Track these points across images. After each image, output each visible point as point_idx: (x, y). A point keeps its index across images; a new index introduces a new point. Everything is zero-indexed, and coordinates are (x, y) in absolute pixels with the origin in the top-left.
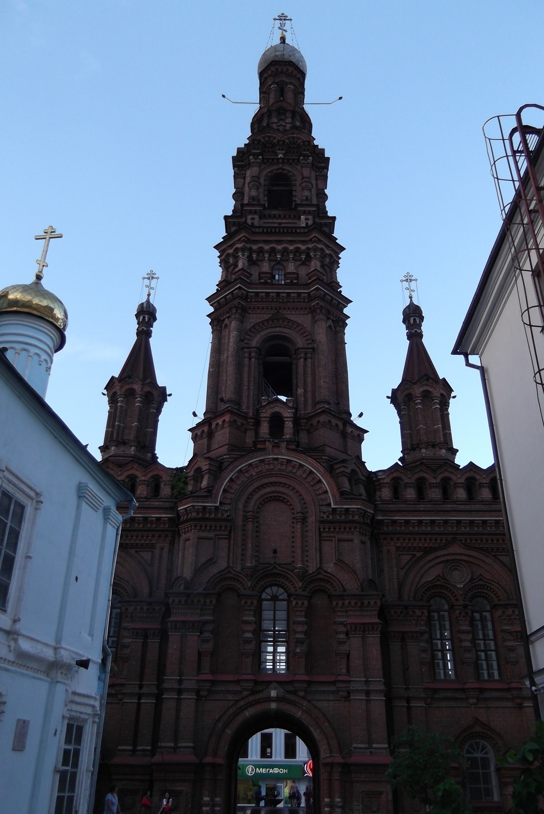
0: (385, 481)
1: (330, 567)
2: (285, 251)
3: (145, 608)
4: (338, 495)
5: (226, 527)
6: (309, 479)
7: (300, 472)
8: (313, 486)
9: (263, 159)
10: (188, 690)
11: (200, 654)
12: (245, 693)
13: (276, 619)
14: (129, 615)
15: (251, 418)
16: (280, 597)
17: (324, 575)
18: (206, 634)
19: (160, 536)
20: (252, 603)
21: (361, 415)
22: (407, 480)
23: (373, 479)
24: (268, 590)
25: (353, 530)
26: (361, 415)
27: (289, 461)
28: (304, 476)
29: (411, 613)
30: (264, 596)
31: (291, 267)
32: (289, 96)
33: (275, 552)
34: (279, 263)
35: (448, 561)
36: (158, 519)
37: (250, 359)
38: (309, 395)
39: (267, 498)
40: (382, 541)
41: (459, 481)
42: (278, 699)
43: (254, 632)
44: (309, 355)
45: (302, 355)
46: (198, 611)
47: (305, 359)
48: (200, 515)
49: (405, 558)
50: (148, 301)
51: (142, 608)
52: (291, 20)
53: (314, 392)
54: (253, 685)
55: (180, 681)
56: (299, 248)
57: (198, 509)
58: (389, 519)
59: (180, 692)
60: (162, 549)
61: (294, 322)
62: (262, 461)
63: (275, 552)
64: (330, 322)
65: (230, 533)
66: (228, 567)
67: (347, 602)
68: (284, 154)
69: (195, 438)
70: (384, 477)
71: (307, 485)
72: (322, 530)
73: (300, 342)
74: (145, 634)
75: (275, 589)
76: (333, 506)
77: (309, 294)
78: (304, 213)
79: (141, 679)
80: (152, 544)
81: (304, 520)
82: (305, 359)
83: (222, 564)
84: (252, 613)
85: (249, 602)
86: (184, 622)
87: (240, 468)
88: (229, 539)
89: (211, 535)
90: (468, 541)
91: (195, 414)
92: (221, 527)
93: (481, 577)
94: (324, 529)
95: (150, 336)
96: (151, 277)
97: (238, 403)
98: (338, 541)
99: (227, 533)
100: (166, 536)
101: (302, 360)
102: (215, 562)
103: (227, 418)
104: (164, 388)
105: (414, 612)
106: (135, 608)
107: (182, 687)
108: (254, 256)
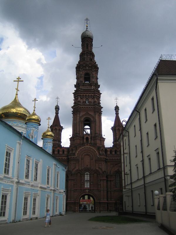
1: (97, 169)
11: (74, 185)
21: (104, 136)
23: (106, 150)
26: (104, 136)
31: (90, 100)
32: (89, 48)
34: (87, 99)
36: (64, 159)
42: (88, 192)
49: (112, 166)
50: (57, 105)
52: (89, 20)
55: (71, 189)
63: (87, 166)
69: (70, 140)
73: (92, 119)
83: (77, 168)
96: (58, 98)
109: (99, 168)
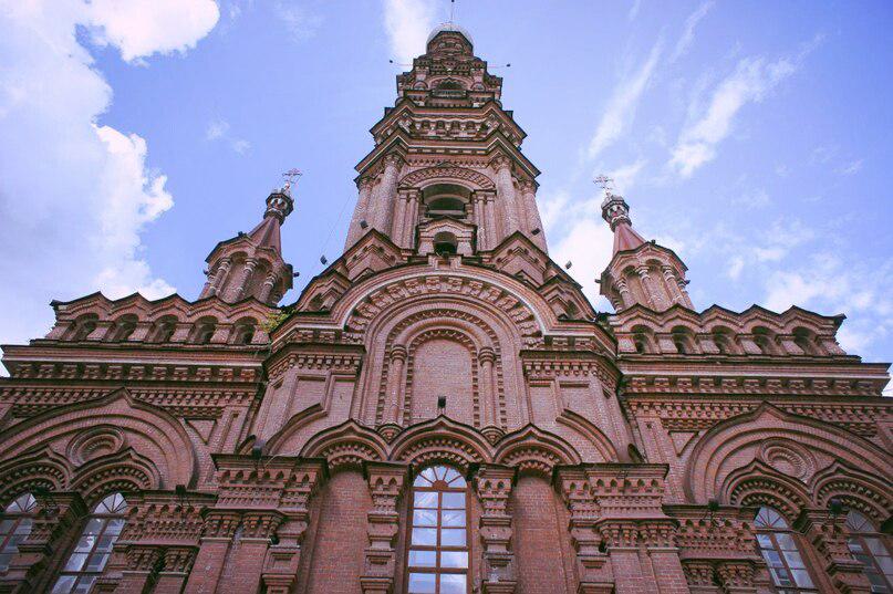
0: (622, 330)
1: (552, 427)
4: (553, 321)
5: (352, 361)
6: (502, 302)
7: (485, 294)
8: (508, 311)
13: (443, 525)
14: (137, 523)
15: (406, 250)
16: (450, 486)
17: (539, 439)
20: (393, 482)
21: (568, 266)
24: (428, 473)
25: (585, 368)
27: (466, 281)
29: (722, 524)
30: (419, 482)
33: (442, 403)
36: (237, 371)
37: (408, 201)
39: (428, 333)
40: (634, 408)
41: (742, 331)
43: (393, 541)
46: (276, 495)
47: (485, 203)
51: (166, 508)
57: (305, 335)
58: (640, 376)
60: (236, 416)
62: (422, 280)
63: (442, 403)
64: (515, 180)
65: (358, 373)
66: (351, 420)
67: (593, 481)
70: (619, 323)
72: (529, 368)
75: (441, 471)
76: (545, 333)
78: (477, 100)
80: (221, 408)
81: (494, 359)
82: (485, 203)
83: (337, 417)
84: (391, 502)
85: (386, 480)
86: (241, 513)
88: (355, 380)
89: (325, 372)
91: (324, 261)
92: (343, 361)
94: (533, 367)
98: (562, 386)
99: (353, 369)
100: (246, 396)
101: (481, 202)
102: (326, 415)
104: (290, 267)
105: (728, 524)
108: (418, 126)
109: (569, 417)
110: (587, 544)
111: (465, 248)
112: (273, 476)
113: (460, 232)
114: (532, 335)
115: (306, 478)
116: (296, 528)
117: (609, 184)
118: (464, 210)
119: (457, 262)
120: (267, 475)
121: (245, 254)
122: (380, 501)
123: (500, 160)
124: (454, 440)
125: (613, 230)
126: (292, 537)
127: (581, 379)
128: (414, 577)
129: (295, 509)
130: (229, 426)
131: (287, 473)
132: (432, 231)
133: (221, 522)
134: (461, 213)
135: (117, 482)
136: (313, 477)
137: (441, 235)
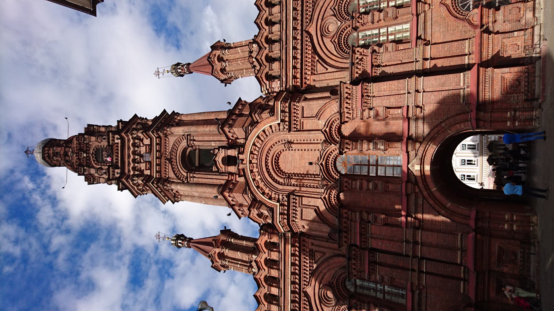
2: (134, 153)
3: (353, 262)
9: (86, 166)
10: (414, 236)
11: (386, 225)
12: (417, 190)
15: (229, 177)
18: (370, 218)
19: (304, 245)
20: (346, 182)
21: (230, 103)
22: (267, 69)
26: (230, 103)
28: (260, 142)
31: (143, 150)
33: (311, 164)
35: (322, 35)
37: (195, 177)
38: (216, 138)
41: (267, 30)
43: (368, 181)
44: (192, 138)
45: (192, 142)
46: (353, 223)
47: (194, 140)
48: (286, 217)
49: (320, 68)
51: (354, 264)
53: (214, 135)
54: (410, 184)
55: (407, 242)
56: (132, 144)
57: (282, 218)
59: (416, 243)
60: (312, 244)
61: (173, 148)
63: (311, 164)
68: (85, 152)
71: (267, 140)
72: (295, 129)
73: (184, 144)
74: (373, 263)
76: (279, 122)
77: (156, 138)
79: (408, 270)
81: (290, 143)
82: (194, 140)
84: (354, 183)
85: (345, 184)
86: (360, 235)
87: (255, 187)
89: (299, 209)
90: (308, 20)
91: (229, 215)
93: (332, 8)
94: (295, 128)
95: (192, 239)
97: (220, 186)
98: (303, 117)
99: (297, 198)
100: (304, 241)
101: (194, 142)
103: (227, 194)
106: (354, 269)
107: (412, 241)
108: (136, 173)
110: (369, 114)
111: (232, 153)
112: (346, 225)
113: (222, 154)
114: (279, 126)
115: (346, 213)
116: (365, 215)
117: (161, 70)
118: (196, 150)
119: (241, 157)
120: (345, 227)
121: (219, 253)
122: (354, 186)
123: (165, 132)
124: (327, 159)
125: (192, 73)
126: (368, 217)
127: (300, 109)
128: (379, 173)
129: (358, 216)
130: (317, 246)
131: (344, 220)
132: (222, 168)
133: (364, 242)
134: (197, 151)
135: (342, 286)
136: (345, 211)
137: (223, 163)
